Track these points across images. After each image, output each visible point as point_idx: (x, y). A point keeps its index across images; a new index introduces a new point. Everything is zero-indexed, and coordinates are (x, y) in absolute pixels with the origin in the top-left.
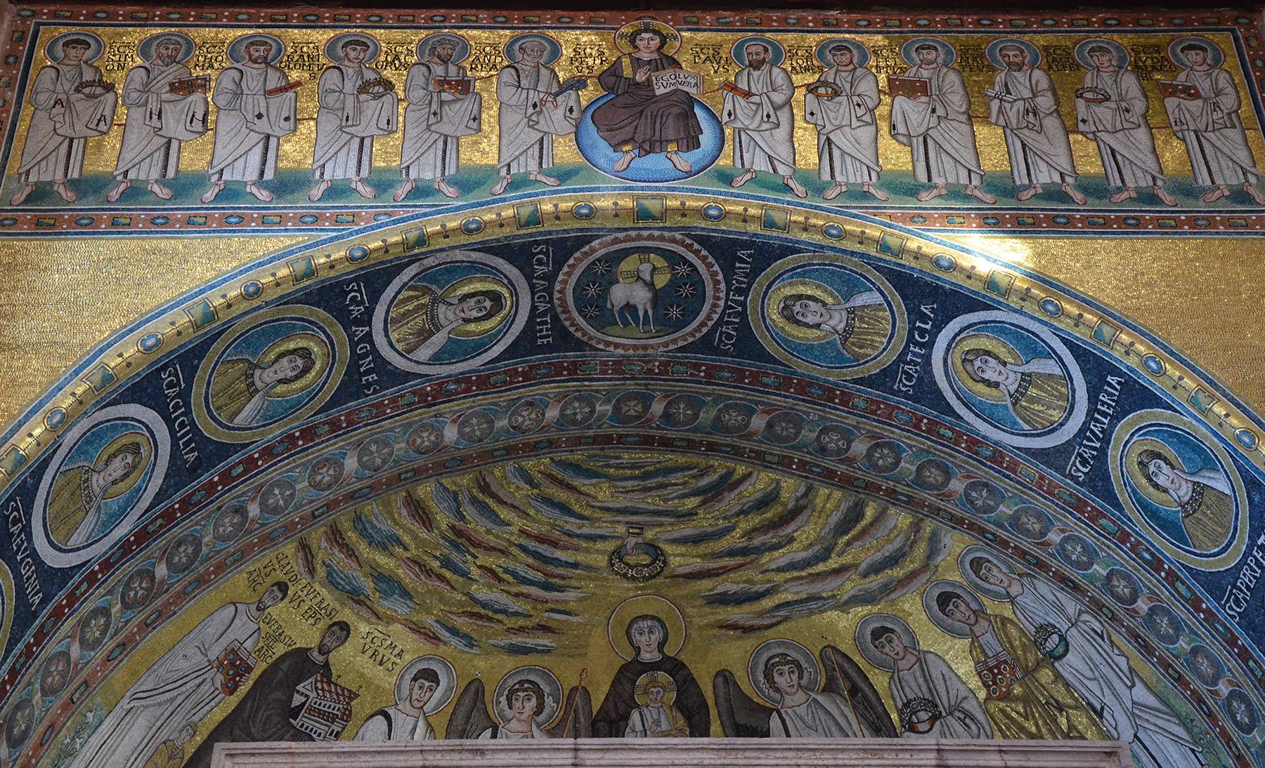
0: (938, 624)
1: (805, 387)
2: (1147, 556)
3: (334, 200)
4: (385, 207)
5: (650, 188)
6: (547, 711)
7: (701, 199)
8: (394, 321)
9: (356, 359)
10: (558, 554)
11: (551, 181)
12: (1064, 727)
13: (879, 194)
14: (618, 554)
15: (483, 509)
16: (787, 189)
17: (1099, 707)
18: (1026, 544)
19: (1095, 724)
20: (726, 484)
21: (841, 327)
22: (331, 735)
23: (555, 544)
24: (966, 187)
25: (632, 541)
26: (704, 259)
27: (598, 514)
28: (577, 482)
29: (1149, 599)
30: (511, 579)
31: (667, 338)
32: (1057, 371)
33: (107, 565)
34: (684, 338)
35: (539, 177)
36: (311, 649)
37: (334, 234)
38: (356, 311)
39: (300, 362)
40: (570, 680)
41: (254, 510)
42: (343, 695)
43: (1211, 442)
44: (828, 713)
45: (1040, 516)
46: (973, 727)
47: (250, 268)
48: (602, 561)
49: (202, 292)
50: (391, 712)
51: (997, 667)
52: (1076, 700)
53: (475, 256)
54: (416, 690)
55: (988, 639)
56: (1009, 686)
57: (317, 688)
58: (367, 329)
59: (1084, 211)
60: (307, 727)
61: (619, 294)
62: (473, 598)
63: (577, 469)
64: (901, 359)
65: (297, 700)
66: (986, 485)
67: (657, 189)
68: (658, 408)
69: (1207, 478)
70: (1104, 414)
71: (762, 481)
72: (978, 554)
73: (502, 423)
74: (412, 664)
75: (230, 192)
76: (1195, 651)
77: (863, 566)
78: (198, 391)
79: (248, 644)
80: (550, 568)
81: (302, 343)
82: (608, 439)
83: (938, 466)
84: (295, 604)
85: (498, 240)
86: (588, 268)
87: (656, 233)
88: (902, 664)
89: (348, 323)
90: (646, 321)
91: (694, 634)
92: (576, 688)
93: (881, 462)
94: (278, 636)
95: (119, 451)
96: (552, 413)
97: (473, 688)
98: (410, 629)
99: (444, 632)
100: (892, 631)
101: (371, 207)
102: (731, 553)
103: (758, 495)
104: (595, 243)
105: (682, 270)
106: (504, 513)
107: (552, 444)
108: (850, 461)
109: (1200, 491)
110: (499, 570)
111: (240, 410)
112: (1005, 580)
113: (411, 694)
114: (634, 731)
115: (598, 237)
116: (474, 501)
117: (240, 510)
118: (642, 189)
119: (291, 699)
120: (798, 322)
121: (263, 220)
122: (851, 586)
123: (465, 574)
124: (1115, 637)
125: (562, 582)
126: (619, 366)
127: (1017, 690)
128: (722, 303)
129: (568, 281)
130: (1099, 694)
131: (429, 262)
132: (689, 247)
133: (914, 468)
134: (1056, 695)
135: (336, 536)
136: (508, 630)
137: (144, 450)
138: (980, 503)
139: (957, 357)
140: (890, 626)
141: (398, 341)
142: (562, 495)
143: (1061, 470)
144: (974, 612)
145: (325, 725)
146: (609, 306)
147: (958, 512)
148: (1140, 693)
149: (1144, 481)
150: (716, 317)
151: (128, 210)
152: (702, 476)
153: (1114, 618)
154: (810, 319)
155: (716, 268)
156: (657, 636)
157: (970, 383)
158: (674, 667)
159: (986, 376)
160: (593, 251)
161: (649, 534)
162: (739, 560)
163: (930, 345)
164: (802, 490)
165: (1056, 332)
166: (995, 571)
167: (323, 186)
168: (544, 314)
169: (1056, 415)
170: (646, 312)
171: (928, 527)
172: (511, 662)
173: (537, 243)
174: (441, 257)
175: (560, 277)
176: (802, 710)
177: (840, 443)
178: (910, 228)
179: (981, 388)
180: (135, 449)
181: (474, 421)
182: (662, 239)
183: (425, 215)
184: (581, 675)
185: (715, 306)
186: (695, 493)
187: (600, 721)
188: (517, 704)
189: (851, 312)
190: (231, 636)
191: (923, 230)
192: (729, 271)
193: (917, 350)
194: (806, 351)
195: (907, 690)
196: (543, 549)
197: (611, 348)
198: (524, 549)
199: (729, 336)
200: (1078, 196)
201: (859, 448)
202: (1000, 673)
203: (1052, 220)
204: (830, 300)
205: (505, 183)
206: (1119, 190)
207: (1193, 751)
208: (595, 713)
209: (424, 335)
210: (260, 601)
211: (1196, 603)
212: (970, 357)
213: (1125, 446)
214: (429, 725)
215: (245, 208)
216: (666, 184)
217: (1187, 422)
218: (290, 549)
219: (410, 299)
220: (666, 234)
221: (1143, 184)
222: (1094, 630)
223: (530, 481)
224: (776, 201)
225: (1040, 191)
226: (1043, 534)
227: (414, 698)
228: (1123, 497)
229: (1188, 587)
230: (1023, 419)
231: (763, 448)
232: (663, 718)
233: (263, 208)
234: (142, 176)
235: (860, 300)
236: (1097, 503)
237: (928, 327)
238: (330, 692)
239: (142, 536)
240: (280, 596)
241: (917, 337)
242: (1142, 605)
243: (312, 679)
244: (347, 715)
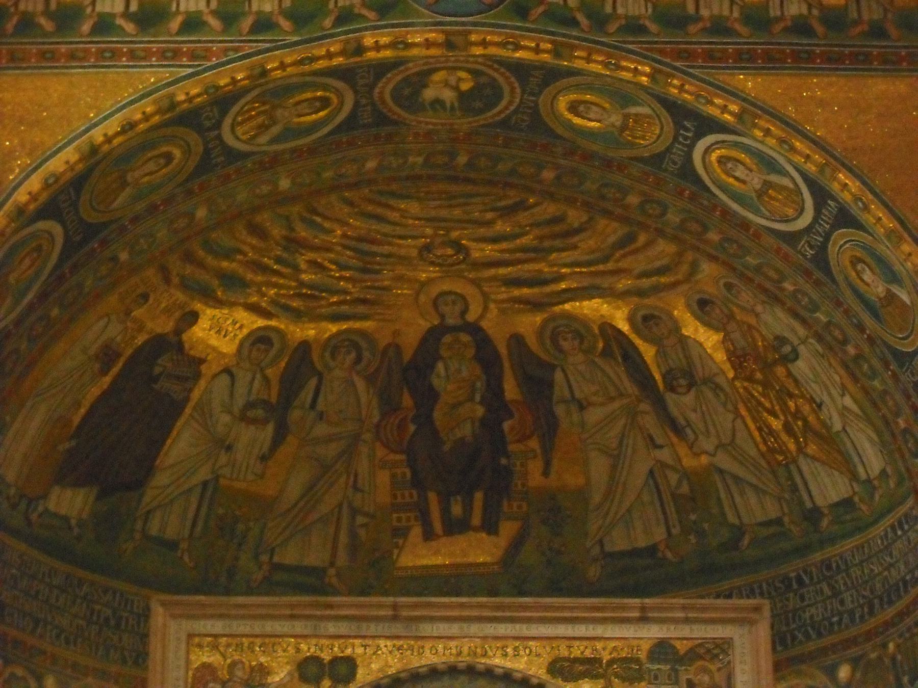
0: (697, 318)
1: (588, 157)
2: (855, 321)
3: (190, 35)
4: (231, 42)
5: (457, 24)
7: (500, 34)
8: (241, 124)
9: (207, 152)
10: (375, 248)
11: (371, 15)
12: (793, 409)
13: (653, 27)
14: (427, 248)
15: (312, 224)
16: (574, 23)
17: (818, 400)
18: (768, 285)
19: (816, 413)
20: (520, 206)
21: (618, 124)
23: (373, 242)
24: (728, 18)
25: (438, 240)
26: (502, 74)
27: (411, 222)
28: (392, 202)
29: (856, 348)
30: (334, 267)
31: (470, 119)
32: (791, 186)
33: (18, 323)
34: (485, 119)
35: (365, 12)
37: (190, 70)
38: (207, 124)
39: (162, 161)
40: (384, 340)
41: (124, 256)
43: (897, 267)
44: (603, 371)
45: (777, 270)
46: (722, 396)
47: (123, 107)
48: (414, 253)
49: (88, 130)
50: (234, 370)
51: (745, 355)
52: (802, 392)
53: (308, 79)
55: (736, 336)
56: (753, 371)
58: (216, 132)
59: (825, 45)
61: (429, 94)
62: (302, 284)
63: (393, 194)
64: (668, 150)
65: (157, 370)
66: (736, 242)
67: (463, 24)
68: (462, 159)
69: (895, 289)
70: (828, 223)
71: (550, 209)
72: (730, 280)
73: (328, 174)
74: (249, 335)
75: (104, 25)
76: (885, 392)
77: (636, 272)
78: (85, 197)
80: (368, 259)
81: (164, 149)
82: (419, 177)
83: (697, 221)
85: (328, 68)
86: (405, 80)
87: (462, 59)
88: (665, 342)
89: (200, 130)
90: (453, 108)
91: (492, 306)
92: (389, 345)
93: (651, 211)
94: (141, 329)
95: (28, 254)
96: (371, 165)
100: (660, 318)
101: (221, 42)
102: (524, 250)
103: (548, 217)
104: (411, 65)
105: (483, 80)
106: (327, 225)
107: (370, 182)
108: (627, 207)
109: (891, 298)
110: (326, 264)
111: (115, 199)
112: (750, 300)
114: (439, 376)
115: (413, 61)
116: (303, 220)
117: (114, 259)
118: (450, 24)
120: (583, 118)
121: (132, 55)
122: (623, 284)
123: (296, 269)
124: (832, 361)
125: (378, 267)
126: (428, 134)
127: (759, 376)
128: (518, 100)
129: (386, 88)
130: (819, 393)
131: (271, 86)
132: (490, 67)
133: (678, 220)
134: (787, 385)
135: (189, 257)
137: (45, 247)
138: (732, 251)
139: (714, 156)
140: (656, 313)
141: (243, 134)
142: (379, 211)
143: (794, 248)
144: (727, 316)
146: (420, 100)
147: (714, 253)
148: (848, 401)
149: (854, 274)
150: (512, 108)
151: (22, 43)
152: (500, 200)
153: (831, 348)
154: (592, 116)
155: (513, 79)
156: (458, 308)
157: (724, 177)
158: (475, 329)
159: (737, 174)
160: (407, 69)
161: (455, 234)
162: (533, 255)
163: (691, 147)
164: (585, 218)
165: (790, 162)
166: (744, 294)
167: (179, 19)
168: (364, 106)
169: (790, 212)
170: (452, 103)
171: (690, 256)
172: (334, 328)
173: (361, 67)
174: (279, 83)
175: (380, 85)
176: (582, 368)
177: (617, 195)
178: (678, 64)
179: (731, 180)
180: (39, 248)
181: (305, 175)
182: (467, 62)
183: (268, 50)
185: (511, 103)
186: (493, 210)
189: (626, 117)
190: (104, 338)
191: (688, 66)
192: (523, 81)
193: (680, 147)
194: (590, 134)
195: (670, 361)
196: (365, 247)
197: (423, 125)
198: (345, 247)
199: (523, 121)
200: (819, 29)
201: (633, 200)
202: (745, 361)
203: (796, 56)
204: (607, 105)
205: (333, 18)
206: (856, 23)
207: (881, 452)
209: (262, 128)
211: (887, 365)
212: (722, 160)
213: (841, 247)
214: (266, 379)
215: (117, 42)
216: (470, 19)
217: (885, 249)
218: (151, 273)
219: (254, 109)
220: (471, 59)
221: (876, 17)
222: (817, 350)
223: (351, 204)
224: (564, 35)
225: (789, 23)
226: (779, 282)
228: (840, 278)
229: (882, 351)
230: (765, 208)
231: (552, 189)
232: (464, 368)
233: (131, 42)
234: (30, 8)
235: (633, 110)
236: (818, 274)
237: (690, 135)
239: (43, 296)
241: (681, 139)
242: (851, 350)
244: (198, 376)
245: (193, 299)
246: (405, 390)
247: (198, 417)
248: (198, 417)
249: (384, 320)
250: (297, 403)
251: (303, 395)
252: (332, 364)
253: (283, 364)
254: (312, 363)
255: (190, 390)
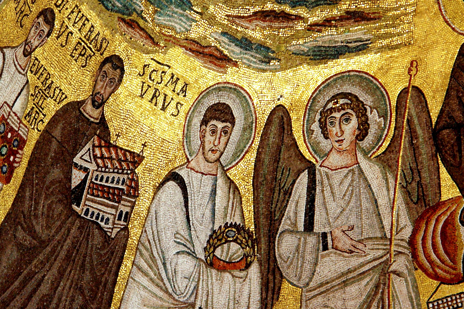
6: (373, 130)
22: (119, 219)
36: (83, 102)
42: (126, 160)
50: (183, 173)
54: (209, 138)
57: (95, 157)
60: (93, 213)
74: (198, 102)
79: (17, 107)
84: (63, 39)
92: (405, 91)
97: (276, 121)
98: (191, 50)
99: (234, 48)
113: (203, 143)
119: (69, 180)
136: (312, 28)
145: (112, 207)
184: (410, 70)
187: (444, 128)
188: (335, 130)
208: (434, 119)
210: (27, 43)
227: (208, 147)
238: (110, 158)
240: (46, 30)
243: (89, 146)
245: (114, 31)
246: (443, 170)
247: (145, 266)
248: (145, 266)
249: (391, 48)
250: (284, 225)
251: (291, 208)
252: (325, 144)
253: (252, 157)
254: (295, 145)
255: (127, 217)
